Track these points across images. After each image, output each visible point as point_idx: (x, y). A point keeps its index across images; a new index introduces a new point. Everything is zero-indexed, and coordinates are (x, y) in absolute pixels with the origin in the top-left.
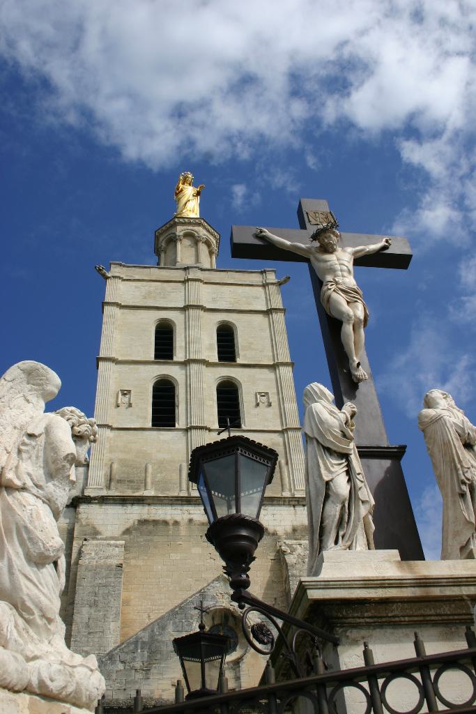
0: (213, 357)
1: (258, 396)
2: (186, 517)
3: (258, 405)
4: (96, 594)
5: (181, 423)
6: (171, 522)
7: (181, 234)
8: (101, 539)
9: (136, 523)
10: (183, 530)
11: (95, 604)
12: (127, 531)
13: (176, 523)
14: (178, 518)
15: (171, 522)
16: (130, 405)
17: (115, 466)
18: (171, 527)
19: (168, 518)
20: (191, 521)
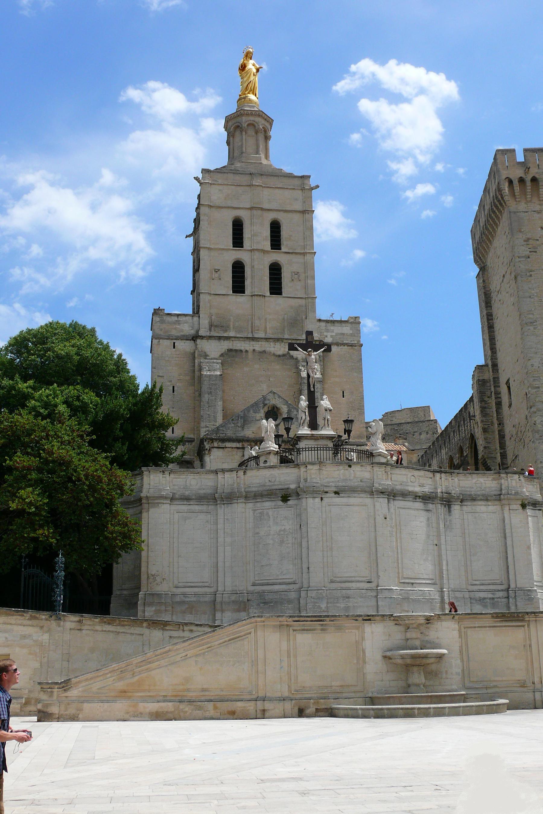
0: (267, 245)
1: (293, 274)
2: (252, 348)
3: (293, 280)
4: (211, 389)
5: (248, 291)
6: (244, 351)
7: (246, 125)
8: (209, 359)
9: (226, 351)
10: (250, 355)
11: (210, 393)
12: (222, 355)
13: (247, 351)
14: (248, 349)
15: (244, 351)
16: (220, 279)
17: (213, 317)
18: (244, 353)
19: (242, 348)
20: (254, 350)
